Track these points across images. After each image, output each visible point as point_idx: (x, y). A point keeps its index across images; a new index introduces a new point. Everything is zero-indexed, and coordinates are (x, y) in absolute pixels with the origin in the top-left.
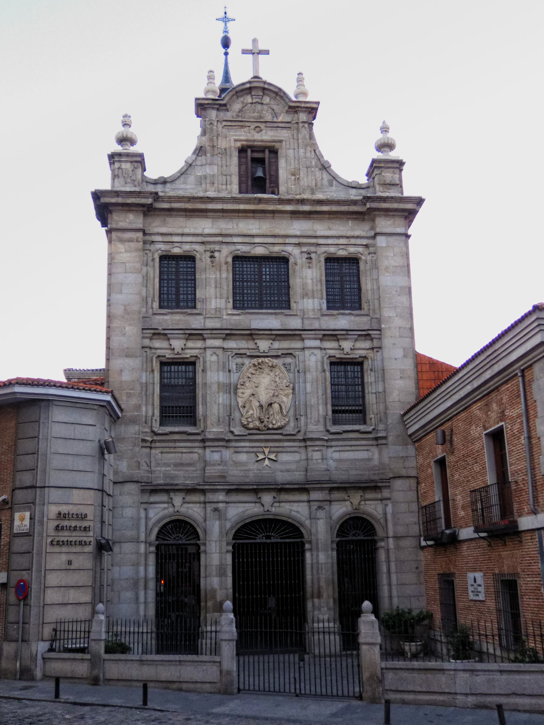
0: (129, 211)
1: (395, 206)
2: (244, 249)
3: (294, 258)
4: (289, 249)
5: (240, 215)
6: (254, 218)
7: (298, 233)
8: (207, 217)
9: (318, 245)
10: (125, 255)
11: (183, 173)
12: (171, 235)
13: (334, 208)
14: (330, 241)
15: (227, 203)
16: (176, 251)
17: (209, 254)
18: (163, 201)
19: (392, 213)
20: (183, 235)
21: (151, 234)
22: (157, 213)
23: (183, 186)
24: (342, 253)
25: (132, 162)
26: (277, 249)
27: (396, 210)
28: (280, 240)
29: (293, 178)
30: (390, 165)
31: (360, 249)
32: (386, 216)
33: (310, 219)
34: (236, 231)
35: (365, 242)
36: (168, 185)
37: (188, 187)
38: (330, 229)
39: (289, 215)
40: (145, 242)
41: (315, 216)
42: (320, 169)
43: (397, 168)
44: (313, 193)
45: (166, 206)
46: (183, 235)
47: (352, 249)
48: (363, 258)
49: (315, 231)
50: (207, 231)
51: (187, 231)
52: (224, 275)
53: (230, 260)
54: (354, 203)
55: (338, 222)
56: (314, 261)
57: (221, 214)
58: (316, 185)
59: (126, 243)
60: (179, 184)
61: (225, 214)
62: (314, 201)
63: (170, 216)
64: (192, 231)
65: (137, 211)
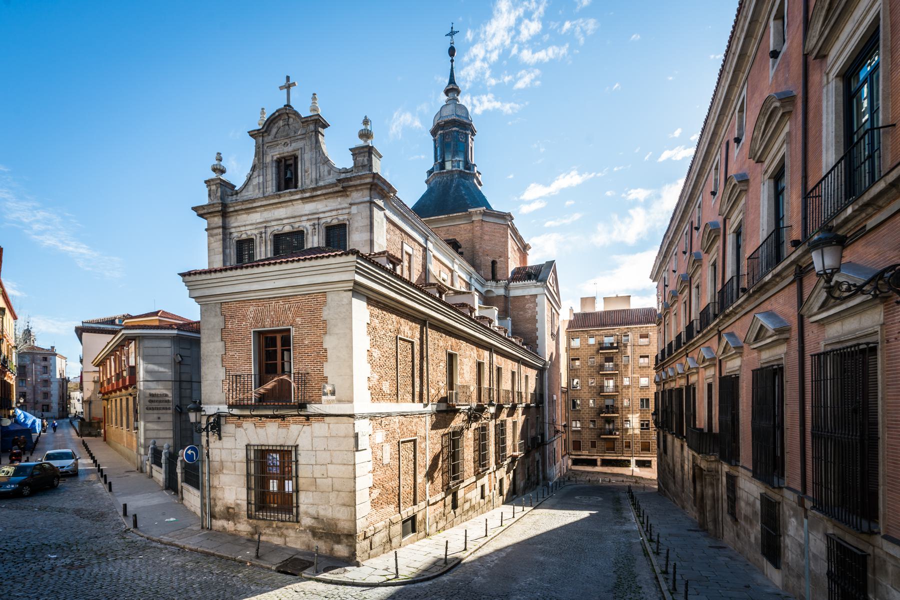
0: (214, 216)
1: (358, 182)
2: (277, 228)
3: (307, 230)
4: (304, 224)
5: (274, 207)
6: (282, 207)
7: (307, 212)
8: (256, 212)
9: (319, 219)
10: (215, 244)
11: (246, 185)
12: (239, 227)
13: (324, 191)
14: (327, 214)
15: (263, 201)
16: (244, 237)
17: (258, 236)
18: (230, 207)
19: (360, 188)
20: (245, 226)
21: (229, 229)
22: (231, 214)
23: (246, 194)
24: (335, 222)
25: (215, 185)
26: (296, 225)
27: (360, 185)
28: (297, 219)
29: (306, 174)
30: (362, 151)
31: (346, 217)
32: (357, 190)
33: (314, 201)
34: (273, 218)
35: (347, 211)
36: (239, 195)
37: (249, 193)
38: (326, 206)
39: (301, 201)
40: (224, 234)
41: (316, 199)
42: (323, 164)
43: (366, 152)
44: (317, 181)
45: (232, 209)
46: (245, 226)
47: (341, 218)
48: (348, 223)
49: (318, 209)
50: (258, 221)
51: (247, 223)
52: (269, 248)
53: (272, 237)
54: (335, 185)
55: (332, 200)
56: (317, 230)
57: (263, 209)
58: (320, 176)
59: (215, 237)
60: (244, 193)
61: (266, 208)
62: (310, 189)
63: (239, 215)
64: (251, 222)
65: (218, 216)
